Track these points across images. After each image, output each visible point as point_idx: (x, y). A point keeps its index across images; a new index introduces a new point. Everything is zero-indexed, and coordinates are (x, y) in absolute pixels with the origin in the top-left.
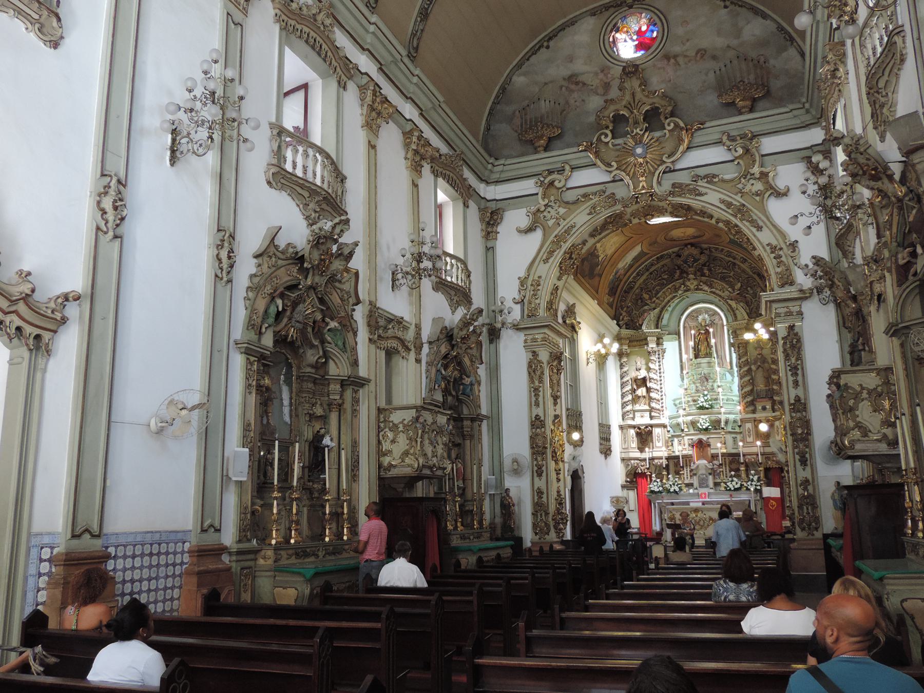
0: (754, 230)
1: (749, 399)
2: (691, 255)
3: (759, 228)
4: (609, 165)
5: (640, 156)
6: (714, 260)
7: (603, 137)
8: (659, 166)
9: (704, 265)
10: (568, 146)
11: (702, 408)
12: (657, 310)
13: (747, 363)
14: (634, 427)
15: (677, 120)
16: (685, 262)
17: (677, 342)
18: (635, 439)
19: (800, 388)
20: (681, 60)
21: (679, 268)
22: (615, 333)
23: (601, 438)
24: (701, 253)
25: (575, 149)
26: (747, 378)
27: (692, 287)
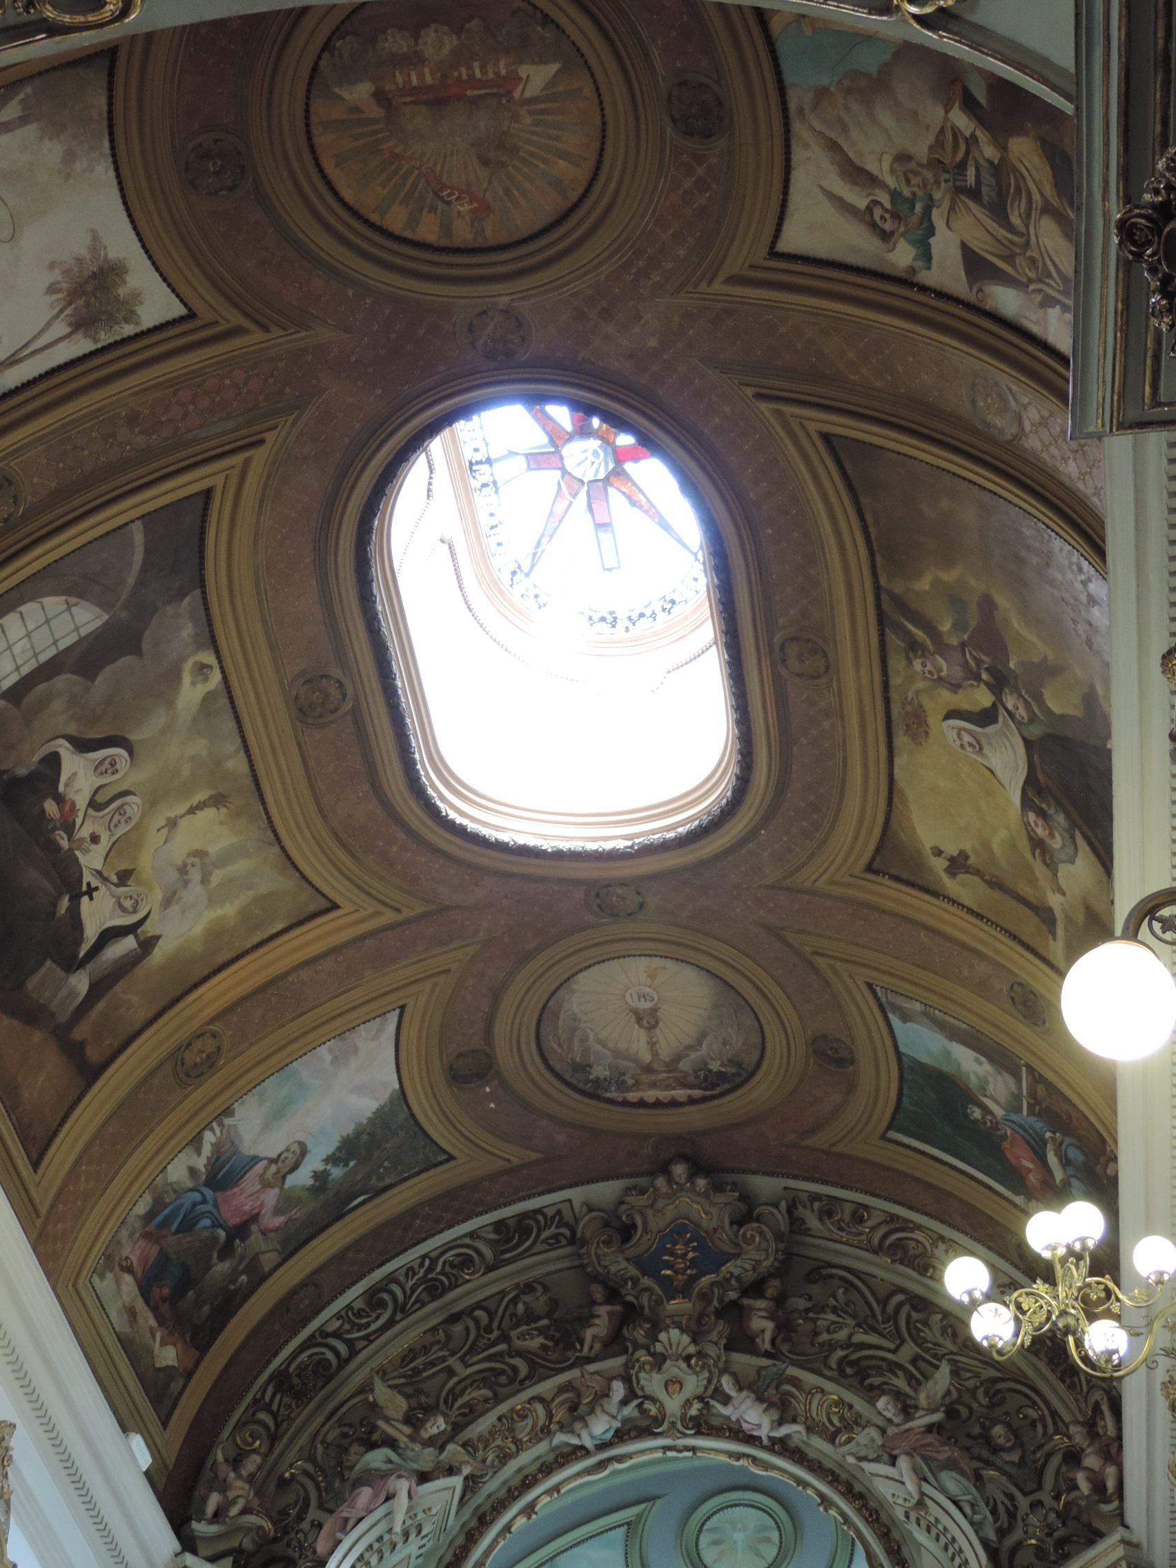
9: (755, 1289)
21: (613, 1295)
24: (739, 1221)
27: (673, 1405)
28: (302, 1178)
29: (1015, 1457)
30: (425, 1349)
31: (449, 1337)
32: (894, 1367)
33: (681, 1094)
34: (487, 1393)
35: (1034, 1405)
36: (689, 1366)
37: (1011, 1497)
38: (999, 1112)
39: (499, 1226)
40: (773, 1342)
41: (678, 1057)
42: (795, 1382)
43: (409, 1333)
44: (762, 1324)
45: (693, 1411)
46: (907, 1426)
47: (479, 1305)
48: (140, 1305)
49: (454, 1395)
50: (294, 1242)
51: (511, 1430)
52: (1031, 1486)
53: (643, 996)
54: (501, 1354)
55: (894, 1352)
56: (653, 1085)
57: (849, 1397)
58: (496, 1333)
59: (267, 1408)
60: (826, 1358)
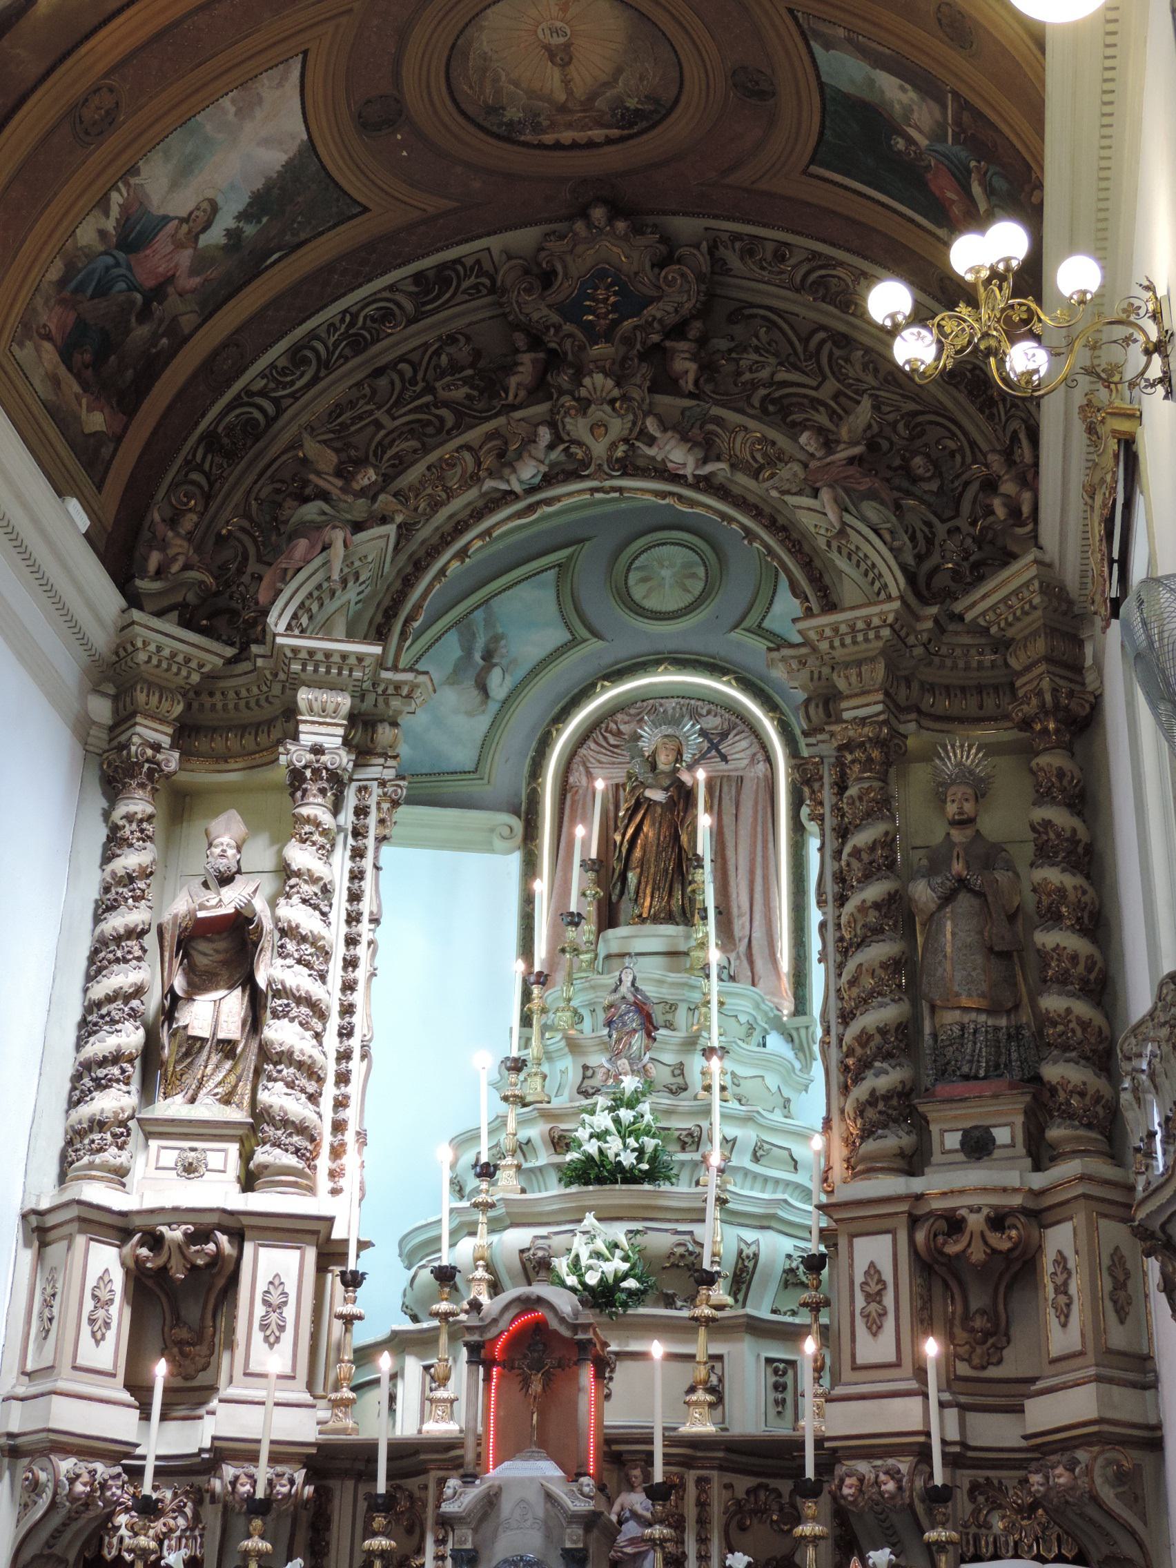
1: (885, 1079)
6: (733, 318)
9: (678, 331)
11: (594, 1172)
13: (881, 860)
14: (117, 1228)
16: (571, 311)
17: (514, 861)
18: (119, 1314)
21: (536, 342)
22: (102, 640)
24: (661, 264)
26: (878, 952)
27: (599, 448)
28: (215, 236)
29: (934, 486)
30: (352, 404)
31: (374, 392)
32: (815, 403)
33: (598, 134)
34: (414, 443)
35: (953, 436)
36: (614, 409)
37: (929, 525)
38: (923, 142)
39: (418, 277)
40: (696, 383)
41: (592, 98)
42: (719, 421)
43: (335, 389)
44: (685, 366)
45: (619, 453)
46: (828, 460)
47: (402, 359)
48: (62, 371)
49: (382, 447)
50: (211, 304)
51: (441, 478)
52: (948, 513)
53: (555, 31)
54: (427, 405)
55: (816, 389)
56: (569, 126)
57: (772, 434)
58: (421, 385)
59: (199, 468)
60: (749, 397)
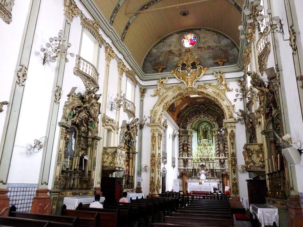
0: (222, 101)
1: (218, 152)
2: (202, 107)
3: (224, 100)
4: (180, 78)
5: (189, 76)
6: (209, 109)
7: (178, 69)
8: (194, 79)
10: (167, 72)
12: (192, 123)
14: (183, 159)
15: (201, 66)
18: (183, 163)
19: (234, 150)
20: (203, 49)
21: (199, 111)
23: (173, 162)
24: (205, 107)
25: (169, 72)
27: (202, 117)
32: (214, 115)
